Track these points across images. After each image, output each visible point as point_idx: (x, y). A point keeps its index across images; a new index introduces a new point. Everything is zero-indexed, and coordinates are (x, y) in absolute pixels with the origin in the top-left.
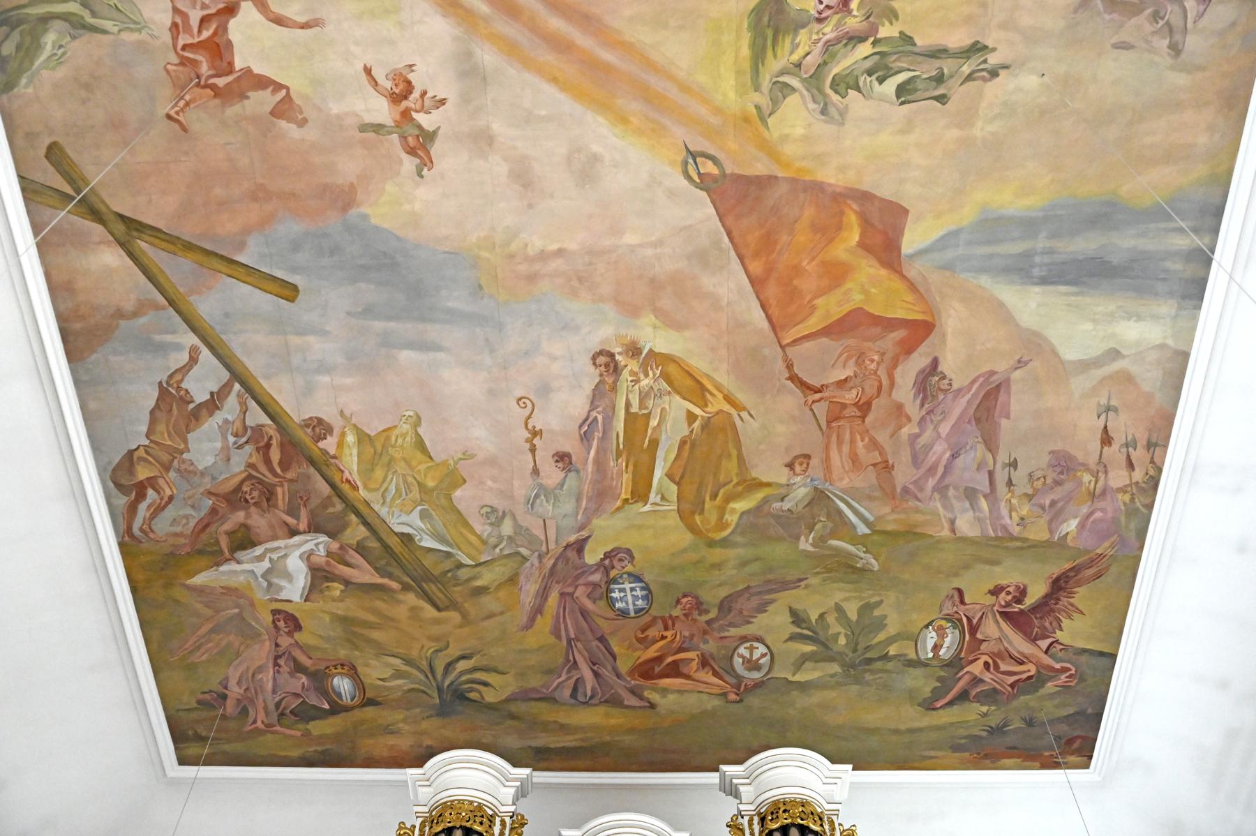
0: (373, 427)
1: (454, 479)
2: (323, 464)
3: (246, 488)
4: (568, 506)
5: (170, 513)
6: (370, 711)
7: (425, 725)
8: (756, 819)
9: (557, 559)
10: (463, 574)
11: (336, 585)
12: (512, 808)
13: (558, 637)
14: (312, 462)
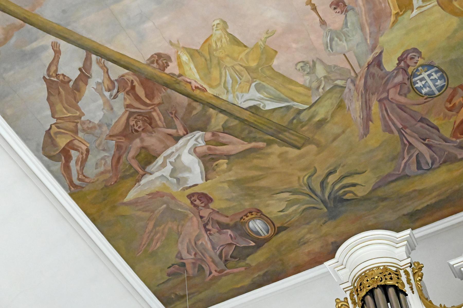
0: (197, 44)
1: (268, 54)
2: (175, 84)
3: (132, 123)
4: (357, 37)
5: (92, 160)
6: (283, 236)
7: (325, 229)
9: (366, 78)
10: (304, 116)
11: (221, 161)
12: (409, 260)
13: (391, 132)
14: (167, 85)
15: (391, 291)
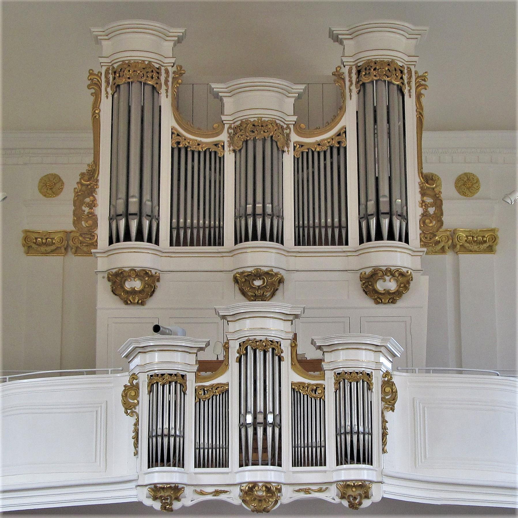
8: (354, 71)
12: (173, 60)
15: (148, 89)
